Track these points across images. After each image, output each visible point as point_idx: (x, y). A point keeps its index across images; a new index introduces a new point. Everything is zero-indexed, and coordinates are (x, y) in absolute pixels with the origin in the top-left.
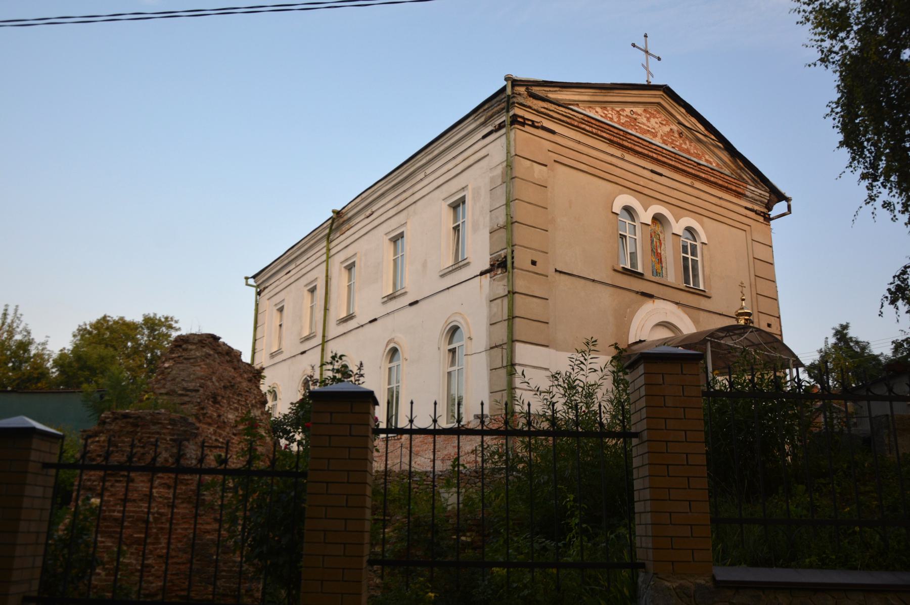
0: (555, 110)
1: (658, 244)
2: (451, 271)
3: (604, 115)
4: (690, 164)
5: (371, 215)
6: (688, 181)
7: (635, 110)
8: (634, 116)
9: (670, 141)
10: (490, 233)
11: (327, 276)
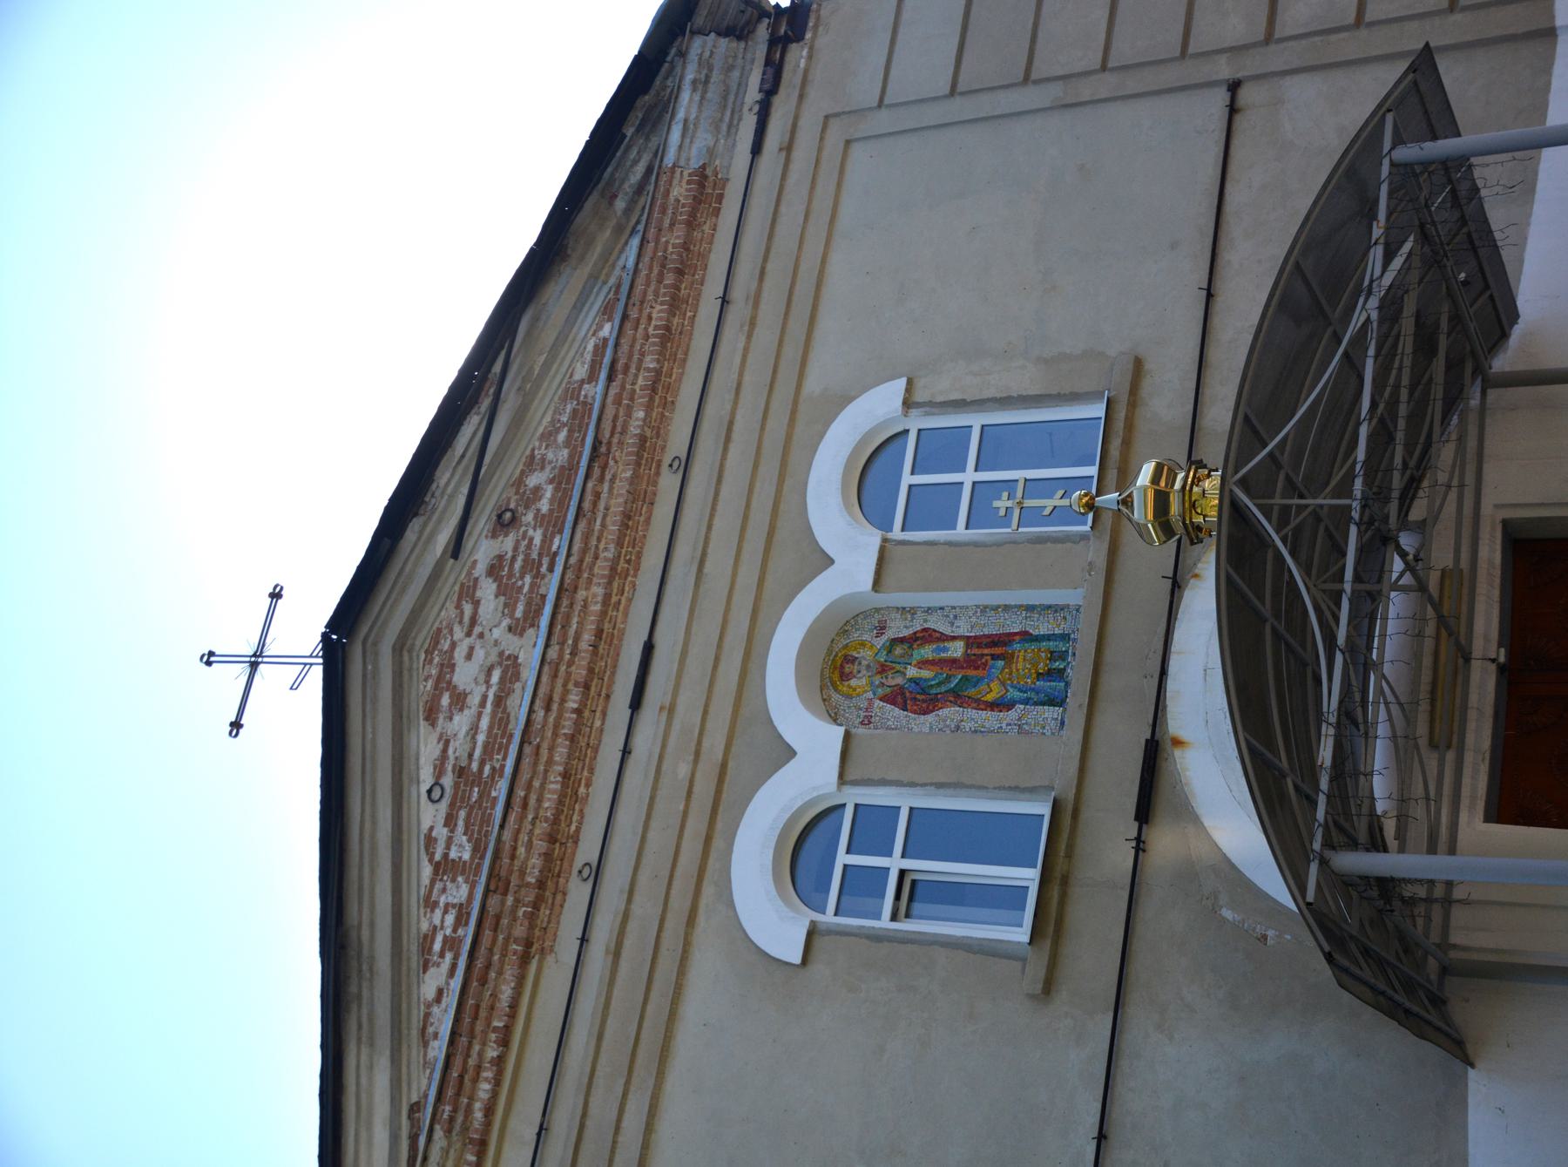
1: (927, 652)
3: (449, 956)
7: (427, 779)
8: (448, 781)
9: (528, 579)
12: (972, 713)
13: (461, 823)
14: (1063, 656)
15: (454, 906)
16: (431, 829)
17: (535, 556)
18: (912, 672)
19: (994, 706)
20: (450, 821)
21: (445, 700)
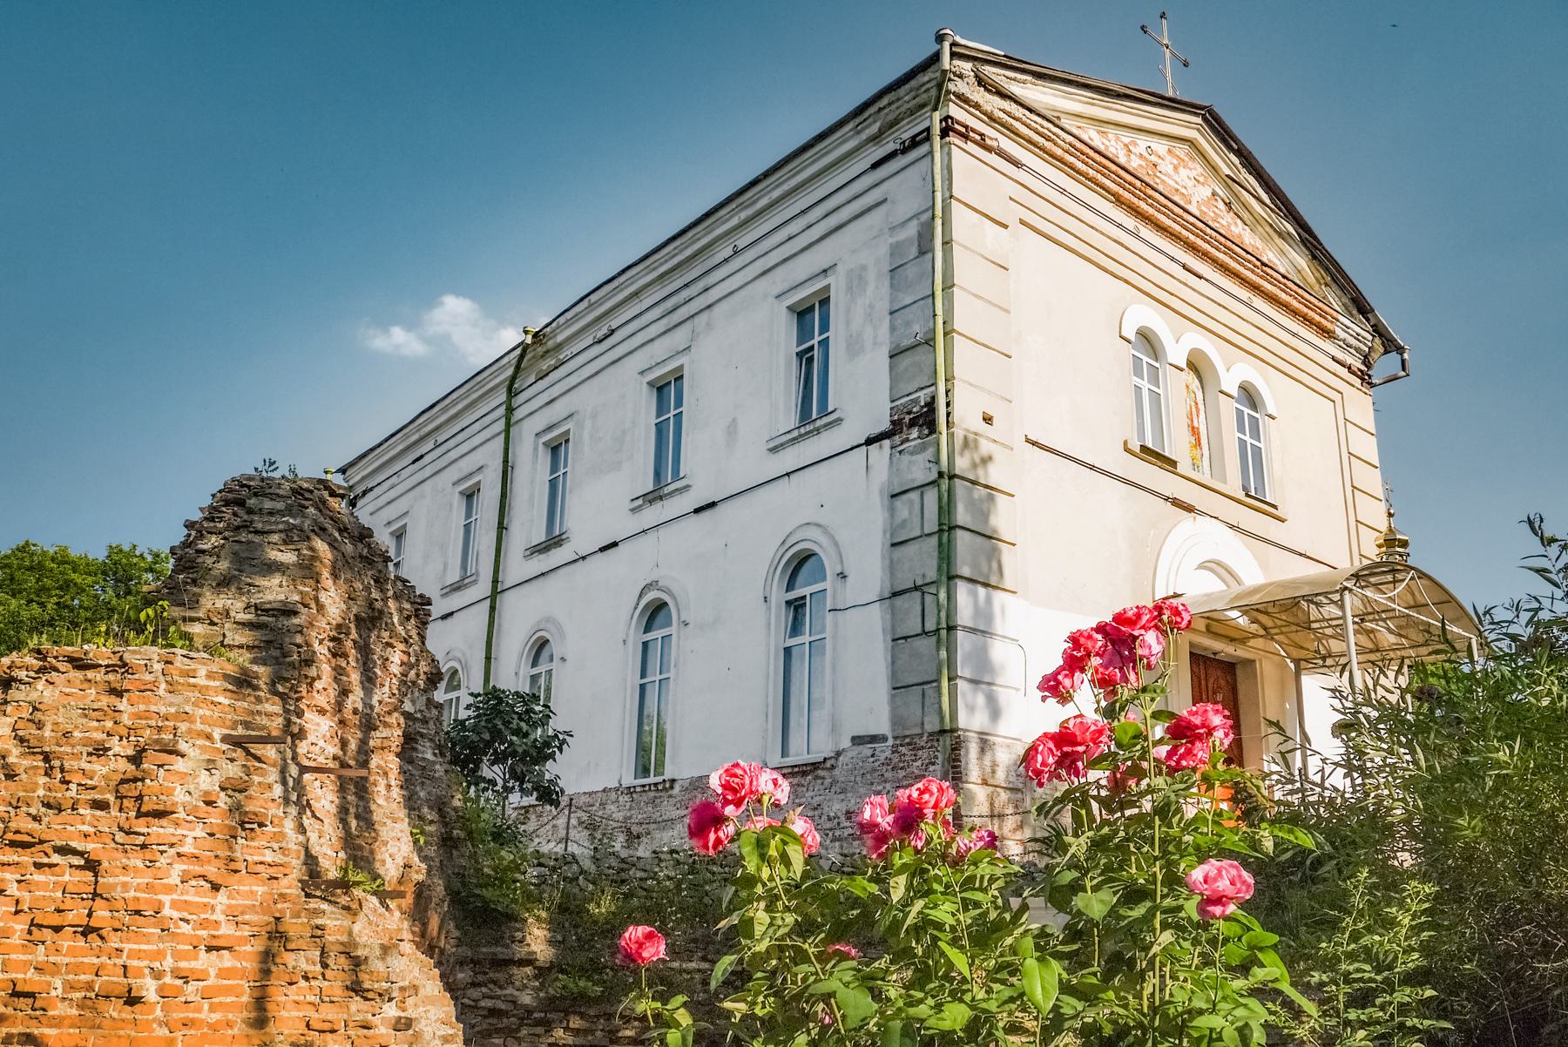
0: (1024, 118)
2: (794, 439)
4: (1249, 262)
5: (606, 337)
6: (1244, 294)
8: (1153, 158)
9: (1212, 215)
10: (891, 357)
11: (506, 461)
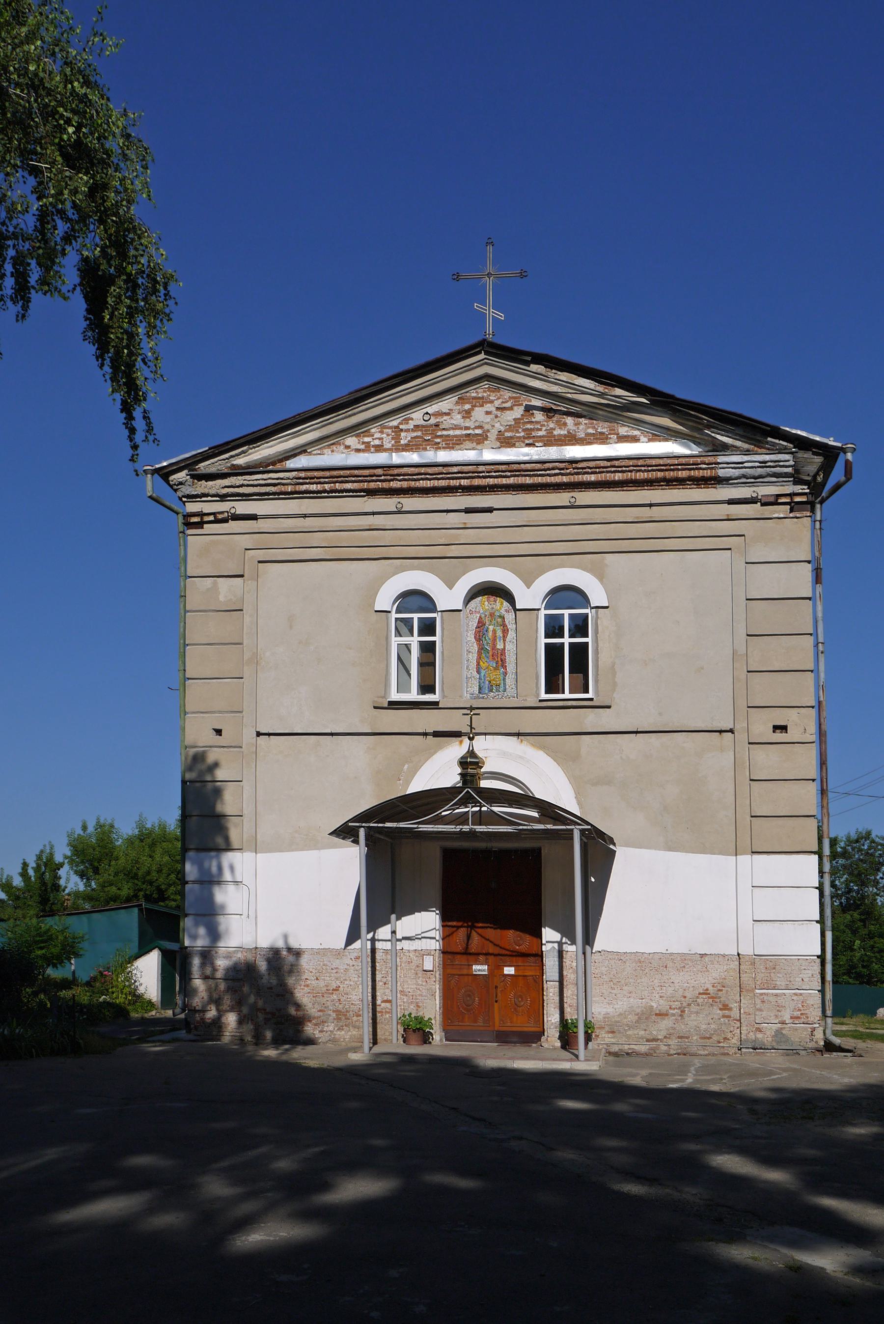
0: (246, 483)
1: (499, 633)
3: (363, 447)
4: (553, 469)
6: (563, 498)
7: (430, 410)
8: (433, 421)
12: (475, 655)
13: (415, 434)
14: (498, 691)
15: (382, 442)
16: (412, 419)
17: (534, 434)
18: (491, 628)
19: (478, 664)
20: (417, 427)
21: (467, 407)
